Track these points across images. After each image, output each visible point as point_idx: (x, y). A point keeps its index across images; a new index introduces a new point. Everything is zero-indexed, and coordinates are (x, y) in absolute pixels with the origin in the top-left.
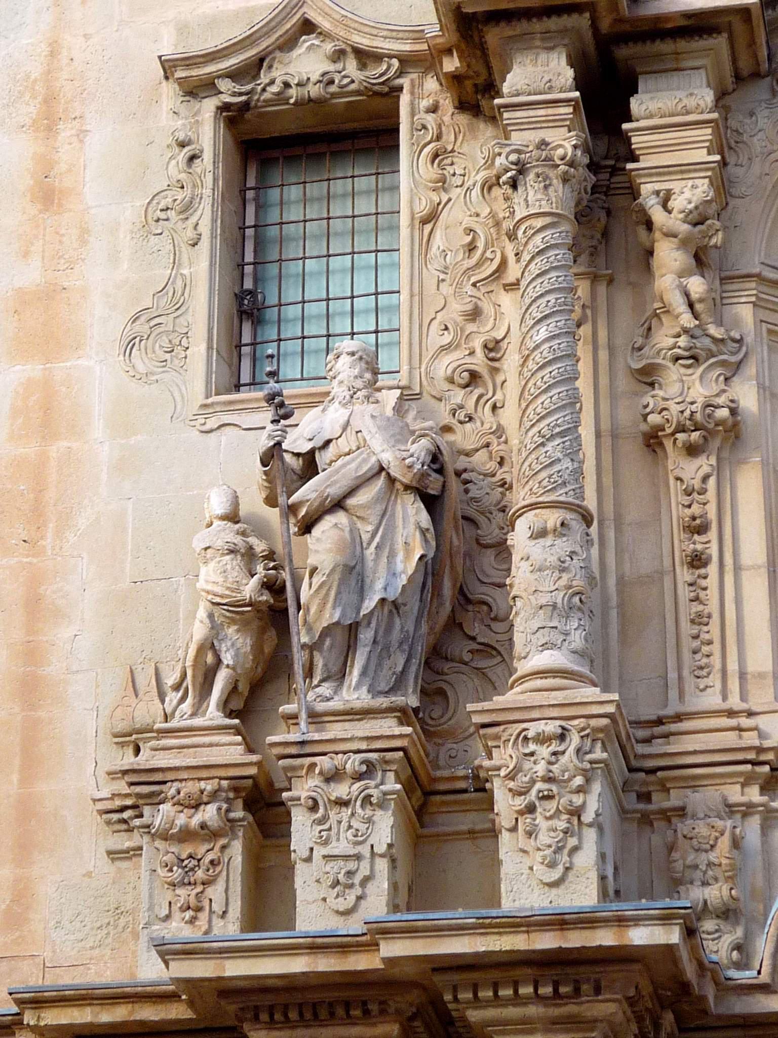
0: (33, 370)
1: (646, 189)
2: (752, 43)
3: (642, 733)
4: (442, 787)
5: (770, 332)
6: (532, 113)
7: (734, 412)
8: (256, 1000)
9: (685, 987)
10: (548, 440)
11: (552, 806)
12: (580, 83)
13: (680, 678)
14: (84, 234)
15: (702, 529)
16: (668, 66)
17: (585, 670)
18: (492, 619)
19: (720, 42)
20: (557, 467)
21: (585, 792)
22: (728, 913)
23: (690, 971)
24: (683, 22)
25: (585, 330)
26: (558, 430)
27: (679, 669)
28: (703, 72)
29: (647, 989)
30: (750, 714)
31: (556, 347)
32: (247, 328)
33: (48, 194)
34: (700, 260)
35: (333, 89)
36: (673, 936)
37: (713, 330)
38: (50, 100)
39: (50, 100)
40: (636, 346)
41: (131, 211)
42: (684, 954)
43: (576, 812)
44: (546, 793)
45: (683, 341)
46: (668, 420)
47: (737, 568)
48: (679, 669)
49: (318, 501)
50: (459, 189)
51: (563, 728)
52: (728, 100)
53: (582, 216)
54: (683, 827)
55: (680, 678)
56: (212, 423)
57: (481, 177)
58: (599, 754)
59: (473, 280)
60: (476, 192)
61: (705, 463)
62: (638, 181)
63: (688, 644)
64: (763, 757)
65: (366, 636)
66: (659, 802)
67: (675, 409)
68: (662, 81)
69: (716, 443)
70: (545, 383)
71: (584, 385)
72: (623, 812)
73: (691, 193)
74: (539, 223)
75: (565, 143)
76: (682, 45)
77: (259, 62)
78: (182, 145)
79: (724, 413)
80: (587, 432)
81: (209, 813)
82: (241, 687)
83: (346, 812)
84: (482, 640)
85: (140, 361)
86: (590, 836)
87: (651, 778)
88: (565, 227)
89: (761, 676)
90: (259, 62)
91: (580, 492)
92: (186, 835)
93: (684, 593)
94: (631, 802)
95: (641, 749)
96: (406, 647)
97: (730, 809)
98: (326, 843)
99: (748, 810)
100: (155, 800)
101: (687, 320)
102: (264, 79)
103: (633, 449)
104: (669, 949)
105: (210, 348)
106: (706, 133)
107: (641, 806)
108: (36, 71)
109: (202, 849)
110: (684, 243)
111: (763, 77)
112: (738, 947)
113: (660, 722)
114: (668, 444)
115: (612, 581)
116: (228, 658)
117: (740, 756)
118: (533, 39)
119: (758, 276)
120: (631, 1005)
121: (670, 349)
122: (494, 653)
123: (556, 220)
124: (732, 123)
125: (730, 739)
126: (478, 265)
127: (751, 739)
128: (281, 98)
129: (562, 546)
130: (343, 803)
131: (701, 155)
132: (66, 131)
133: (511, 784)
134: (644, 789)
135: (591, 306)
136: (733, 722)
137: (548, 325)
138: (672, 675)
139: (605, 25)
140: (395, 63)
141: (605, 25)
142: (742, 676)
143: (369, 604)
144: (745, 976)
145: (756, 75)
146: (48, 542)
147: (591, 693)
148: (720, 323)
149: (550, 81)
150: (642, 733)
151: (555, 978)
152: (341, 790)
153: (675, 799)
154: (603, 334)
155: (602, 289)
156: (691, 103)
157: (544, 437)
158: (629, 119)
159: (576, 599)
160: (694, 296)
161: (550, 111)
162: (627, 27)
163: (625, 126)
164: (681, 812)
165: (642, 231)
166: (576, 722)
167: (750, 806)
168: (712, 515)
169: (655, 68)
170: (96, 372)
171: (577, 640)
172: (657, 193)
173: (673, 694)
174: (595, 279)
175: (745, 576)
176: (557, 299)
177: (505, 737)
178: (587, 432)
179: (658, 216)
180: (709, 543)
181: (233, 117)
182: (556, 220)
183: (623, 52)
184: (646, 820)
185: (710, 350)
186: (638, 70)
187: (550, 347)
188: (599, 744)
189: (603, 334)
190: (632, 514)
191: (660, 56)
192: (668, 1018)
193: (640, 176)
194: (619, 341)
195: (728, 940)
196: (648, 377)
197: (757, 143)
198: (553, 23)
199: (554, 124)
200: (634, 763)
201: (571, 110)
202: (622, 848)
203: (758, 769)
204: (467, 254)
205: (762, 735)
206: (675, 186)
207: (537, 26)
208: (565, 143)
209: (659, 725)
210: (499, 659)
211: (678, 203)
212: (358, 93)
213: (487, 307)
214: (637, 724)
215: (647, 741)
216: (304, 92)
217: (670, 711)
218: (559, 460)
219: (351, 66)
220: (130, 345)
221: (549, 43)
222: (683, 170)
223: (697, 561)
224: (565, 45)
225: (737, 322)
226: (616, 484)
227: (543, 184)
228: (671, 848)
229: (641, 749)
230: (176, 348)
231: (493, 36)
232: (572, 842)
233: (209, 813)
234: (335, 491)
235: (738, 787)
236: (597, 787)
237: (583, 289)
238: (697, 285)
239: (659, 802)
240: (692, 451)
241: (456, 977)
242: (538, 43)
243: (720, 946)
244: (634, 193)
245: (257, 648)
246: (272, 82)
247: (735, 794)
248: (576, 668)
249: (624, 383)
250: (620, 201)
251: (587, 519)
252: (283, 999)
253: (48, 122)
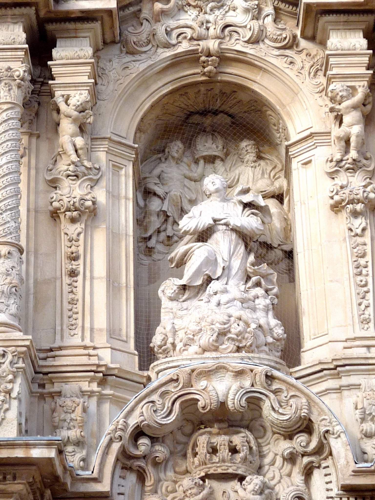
1: (58, 94)
2: (112, 27)
3: (42, 355)
5: (113, 165)
6: (4, 54)
7: (94, 203)
9: (57, 478)
10: (4, 212)
12: (29, 41)
13: (62, 329)
15: (76, 259)
16: (72, 35)
17: (16, 324)
19: (97, 25)
20: (8, 225)
21: (13, 383)
22: (79, 443)
23: (59, 471)
24: (79, 15)
25: (25, 160)
26: (9, 207)
27: (62, 325)
28: (88, 39)
29: (38, 479)
30: (95, 348)
31: (10, 167)
34: (82, 129)
36: (52, 453)
37: (86, 163)
40: (49, 169)
42: (57, 462)
43: (9, 392)
45: (72, 168)
46: (62, 205)
47: (92, 278)
48: (62, 325)
51: (4, 351)
52: (99, 53)
53: (26, 105)
54: (60, 401)
55: (62, 329)
58: (21, 364)
61: (79, 227)
62: (54, 90)
63: (67, 313)
64: (99, 369)
66: (49, 388)
67: (66, 200)
68: (68, 42)
69: (84, 218)
70: (4, 184)
71: (23, 186)
72: (31, 392)
73: (79, 97)
74: (5, 107)
75: (20, 69)
76: (79, 25)
79: (89, 203)
80: (23, 209)
86: (15, 403)
87: (45, 377)
88: (18, 109)
89: (101, 330)
91: (18, 238)
93: (66, 289)
94: (35, 388)
95: (41, 363)
97: (83, 393)
99: (91, 394)
101: (74, 158)
103: (44, 219)
104: (50, 460)
106: (88, 69)
107: (40, 390)
110: (75, 121)
111: (117, 43)
112: (83, 460)
113: (51, 350)
114: (62, 217)
115: (31, 281)
117: (88, 368)
118: (7, 18)
119: (110, 139)
120: (30, 486)
121: (65, 171)
124: (101, 65)
125: (84, 360)
127: (94, 360)
129: (8, 263)
131: (85, 79)
134: (42, 382)
135: (28, 148)
136: (86, 352)
137: (7, 156)
138: (58, 328)
139: (42, 14)
141: (42, 14)
142: (92, 330)
144: (86, 474)
145: (114, 42)
147: (18, 335)
148: (90, 160)
149: (14, 39)
150: (42, 355)
153: (56, 388)
154: (33, 162)
155: (34, 140)
156: (82, 54)
158: (51, 59)
159: (14, 289)
160: (78, 146)
161: (13, 53)
162: (53, 15)
163: (49, 63)
164: (59, 394)
165: (55, 114)
166: (10, 349)
167: (92, 392)
168: (81, 252)
169: (65, 36)
171: (13, 309)
172: (63, 96)
173: (58, 337)
174: (31, 135)
175: (95, 282)
176: (12, 144)
178: (23, 209)
179: (63, 107)
180: (79, 266)
182: (13, 106)
183: (50, 27)
184: (42, 397)
185: (84, 173)
186: (57, 36)
187: (7, 167)
188: (21, 360)
189: (33, 162)
190: (43, 249)
192: (48, 493)
194: (41, 166)
195: (78, 456)
196: (54, 184)
197: (112, 75)
198: (17, 11)
199: (15, 59)
200: (38, 370)
201: (23, 53)
202: (30, 410)
203: (97, 375)
205: (99, 359)
206: (72, 93)
207: (9, 12)
208: (20, 69)
209: (51, 351)
211: (72, 101)
214: (40, 350)
215: (45, 359)
217: (56, 345)
218: (9, 222)
221: (15, 20)
222: (76, 86)
223: (73, 274)
224: (22, 22)
225: (98, 160)
226: (36, 235)
227: (8, 88)
228: (53, 411)
229: (41, 363)
232: (6, 406)
235: (87, 383)
236: (19, 380)
237: (25, 139)
238: (80, 141)
239: (49, 388)
240: (73, 220)
242: (9, 20)
243: (74, 459)
244: (52, 95)
247: (85, 386)
248: (12, 322)
249: (42, 186)
250: (45, 99)
251: (21, 251)
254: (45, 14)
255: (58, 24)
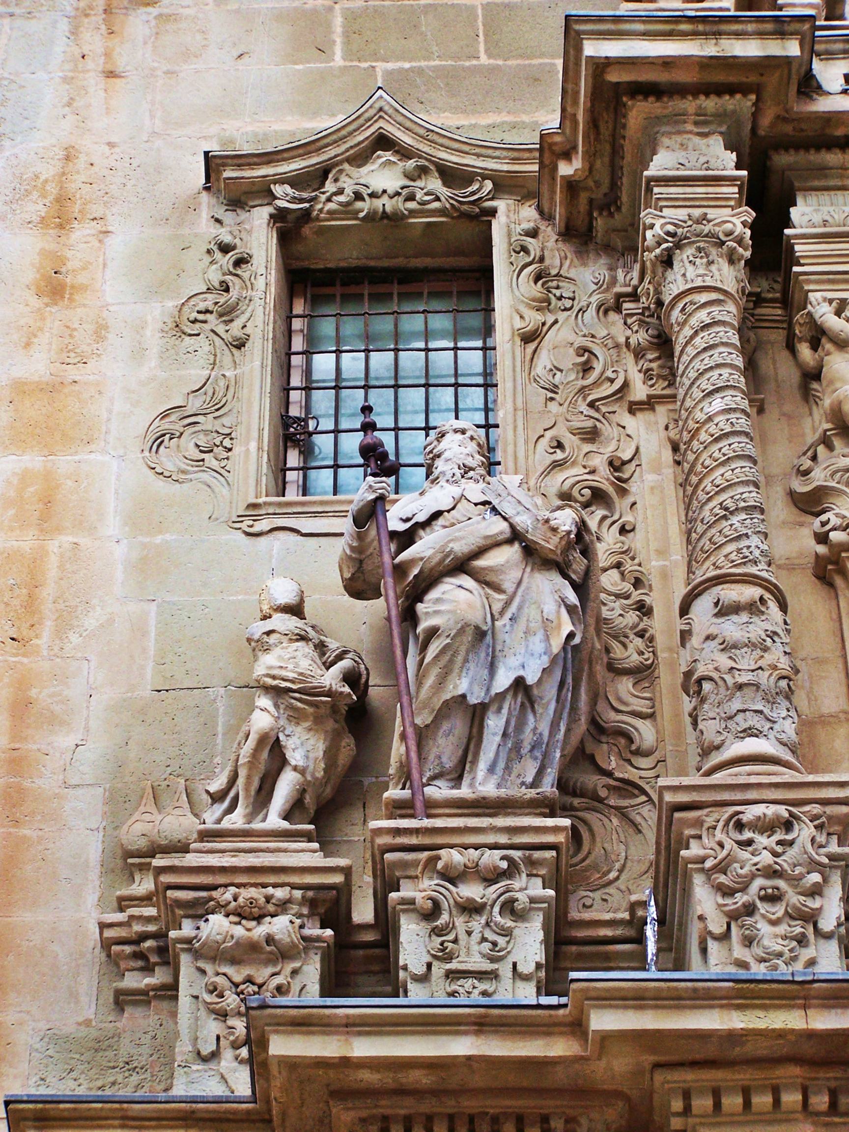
0: (32, 460)
4: (581, 933)
8: (386, 1106)
10: (732, 513)
11: (779, 910)
14: (100, 331)
16: (831, 183)
18: (632, 752)
20: (744, 543)
21: (820, 894)
26: (743, 504)
31: (734, 420)
32: (293, 458)
33: (55, 287)
35: (412, 205)
38: (62, 200)
39: (62, 200)
40: (802, 468)
41: (159, 312)
44: (770, 891)
49: (439, 557)
50: (569, 313)
51: (791, 814)
56: (263, 525)
57: (595, 299)
59: (590, 399)
60: (591, 312)
62: (806, 288)
65: (494, 724)
75: (733, 219)
77: (323, 174)
78: (225, 249)
81: (280, 926)
82: (308, 799)
83: (477, 923)
84: (621, 776)
85: (169, 459)
90: (323, 174)
92: (244, 953)
96: (538, 754)
98: (448, 957)
100: (199, 911)
102: (330, 187)
105: (260, 449)
108: (48, 171)
109: (262, 974)
116: (295, 757)
118: (685, 122)
122: (636, 792)
123: (721, 297)
126: (596, 384)
128: (347, 210)
130: (471, 909)
132: (81, 232)
133: (722, 879)
137: (722, 398)
140: (489, 185)
143: (503, 680)
146: (44, 640)
149: (707, 162)
151: (833, 1084)
152: (472, 891)
157: (726, 509)
162: (788, 129)
163: (787, 231)
166: (807, 808)
169: (816, 183)
170: (111, 470)
172: (831, 301)
176: (731, 374)
177: (709, 821)
181: (289, 228)
182: (721, 297)
186: (796, 184)
187: (728, 420)
188: (835, 838)
191: (822, 170)
193: (809, 282)
201: (736, 190)
204: (581, 375)
208: (733, 219)
210: (643, 798)
212: (442, 212)
213: (605, 429)
216: (378, 204)
218: (747, 536)
219: (435, 184)
220: (159, 441)
221: (705, 124)
224: (721, 133)
227: (705, 260)
230: (220, 446)
231: (638, 112)
233: (280, 926)
234: (461, 548)
241: (689, 1076)
242: (689, 127)
245: (330, 756)
246: (341, 192)
252: (426, 1107)
253: (61, 216)
254: (773, 125)
255: (802, 153)
